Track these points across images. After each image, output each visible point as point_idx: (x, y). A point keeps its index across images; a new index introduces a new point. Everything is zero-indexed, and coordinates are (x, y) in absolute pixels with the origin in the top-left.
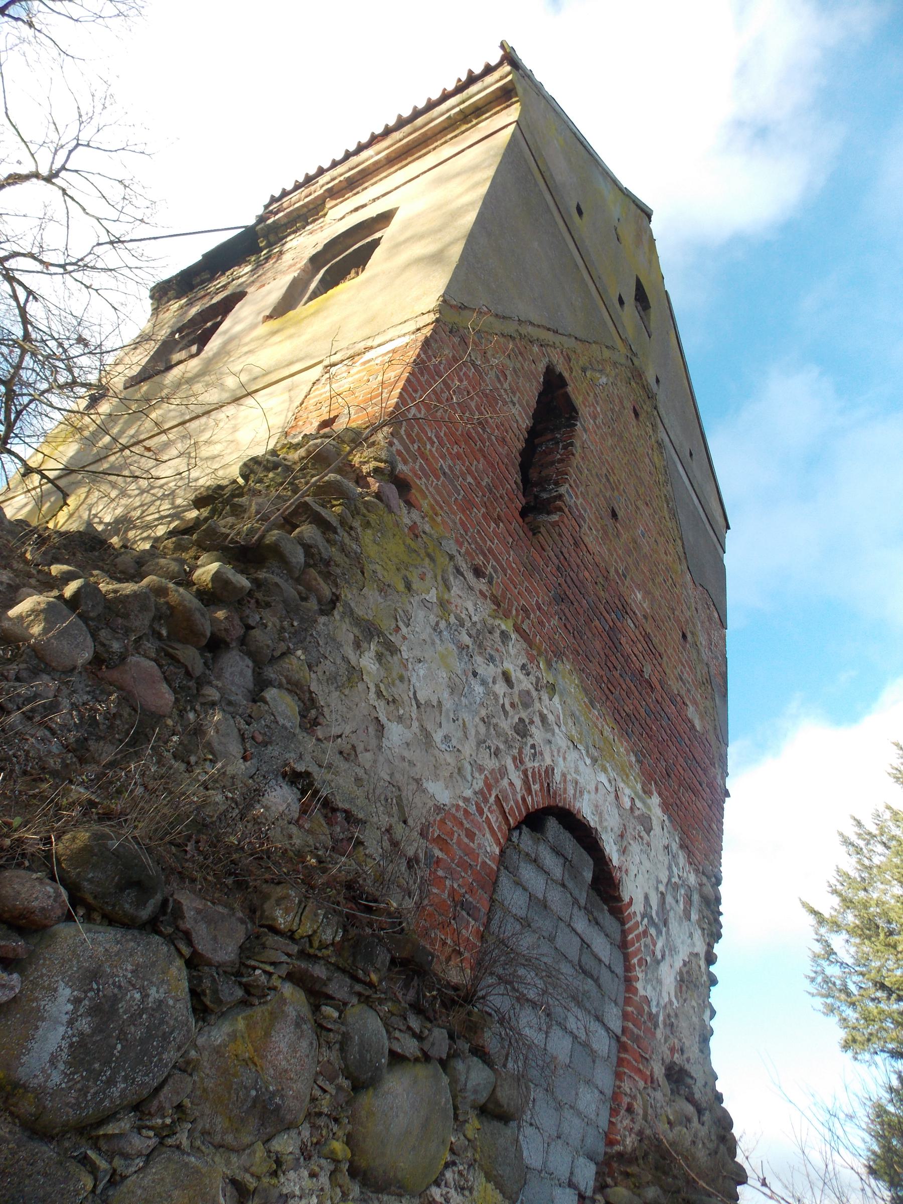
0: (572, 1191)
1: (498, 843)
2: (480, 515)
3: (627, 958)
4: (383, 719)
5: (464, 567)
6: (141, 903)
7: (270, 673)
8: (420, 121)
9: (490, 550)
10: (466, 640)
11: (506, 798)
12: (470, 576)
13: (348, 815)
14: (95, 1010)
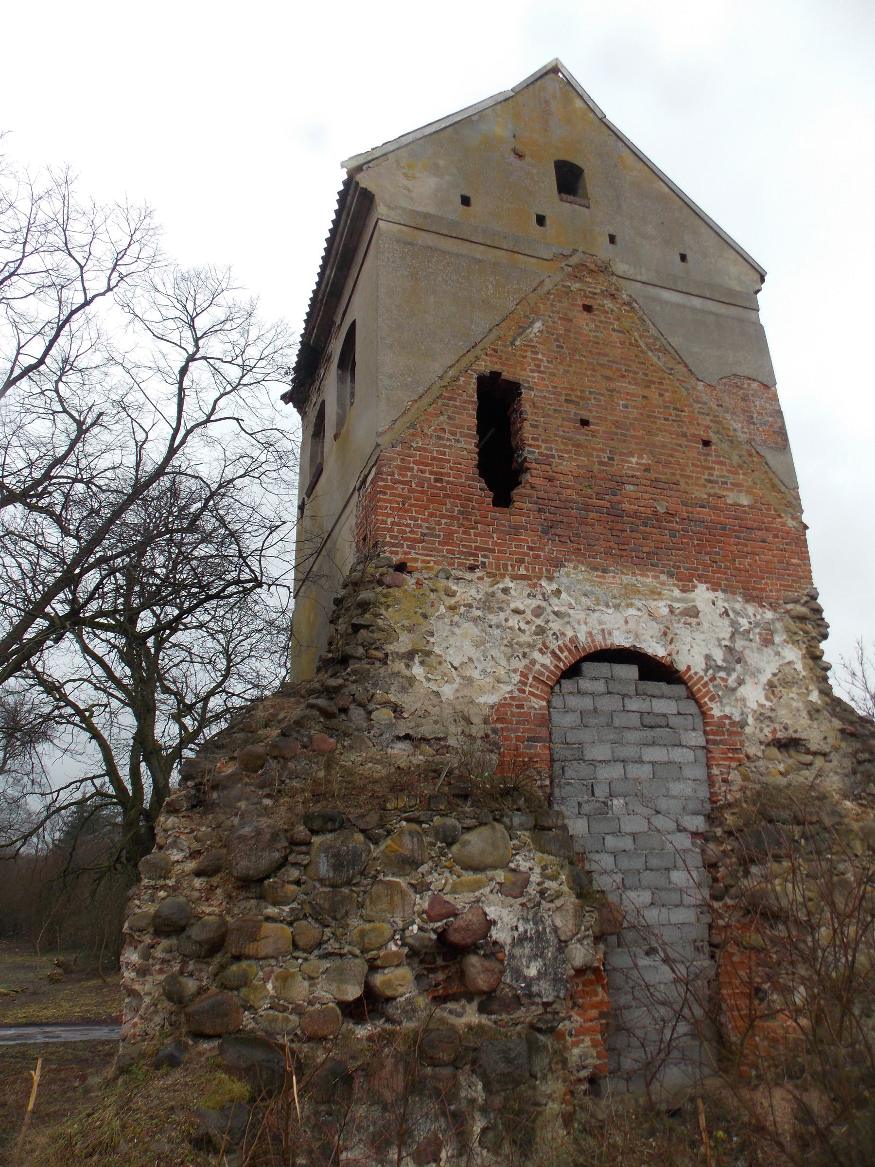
0: (684, 834)
1: (542, 699)
2: (460, 535)
3: (697, 702)
4: (435, 689)
5: (460, 574)
6: (334, 824)
7: (371, 707)
8: (334, 252)
9: (476, 548)
10: (479, 613)
11: (542, 674)
12: (468, 576)
13: (439, 739)
14: (333, 856)
